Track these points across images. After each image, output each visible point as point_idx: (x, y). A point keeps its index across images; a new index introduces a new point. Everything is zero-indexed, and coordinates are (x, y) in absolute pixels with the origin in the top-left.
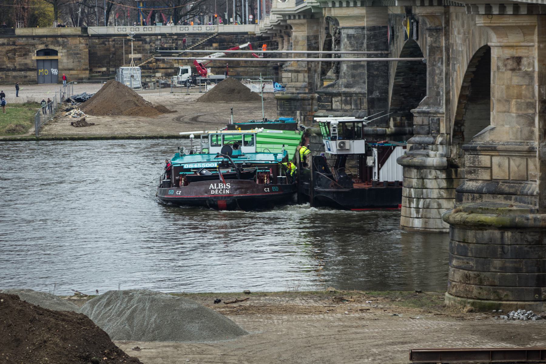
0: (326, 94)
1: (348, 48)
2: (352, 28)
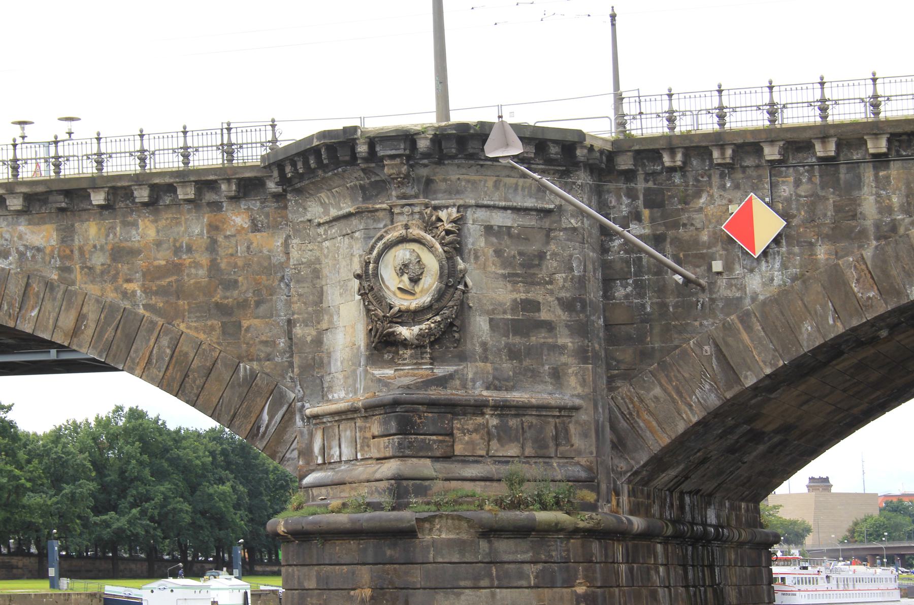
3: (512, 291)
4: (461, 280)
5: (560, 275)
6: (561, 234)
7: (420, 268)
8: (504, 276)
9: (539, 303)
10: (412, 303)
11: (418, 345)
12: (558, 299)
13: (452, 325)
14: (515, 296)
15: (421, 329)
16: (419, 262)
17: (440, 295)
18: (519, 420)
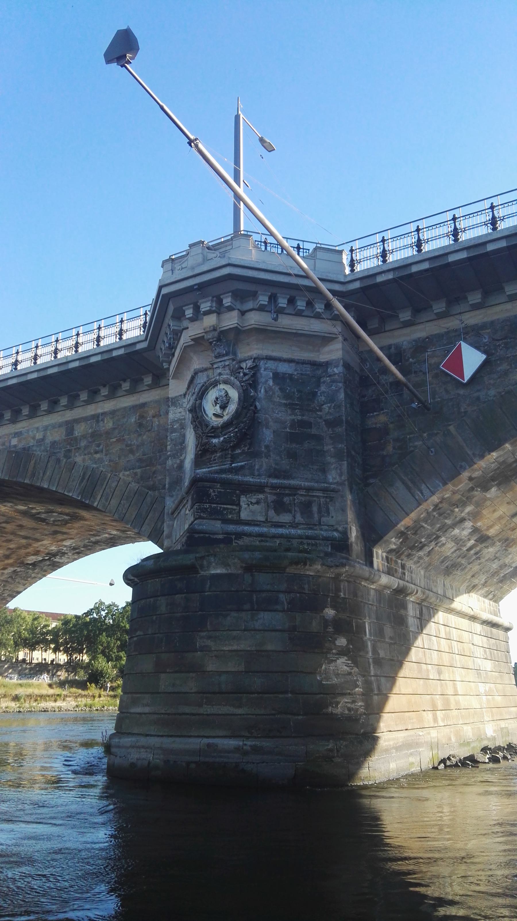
0: (225, 483)
1: (277, 400)
2: (290, 361)
3: (290, 415)
4: (253, 404)
5: (326, 405)
6: (328, 378)
7: (227, 400)
8: (286, 405)
9: (311, 423)
10: (219, 422)
11: (223, 448)
12: (325, 421)
13: (246, 434)
14: (293, 417)
15: (225, 438)
16: (226, 395)
17: (237, 415)
18: (291, 498)
